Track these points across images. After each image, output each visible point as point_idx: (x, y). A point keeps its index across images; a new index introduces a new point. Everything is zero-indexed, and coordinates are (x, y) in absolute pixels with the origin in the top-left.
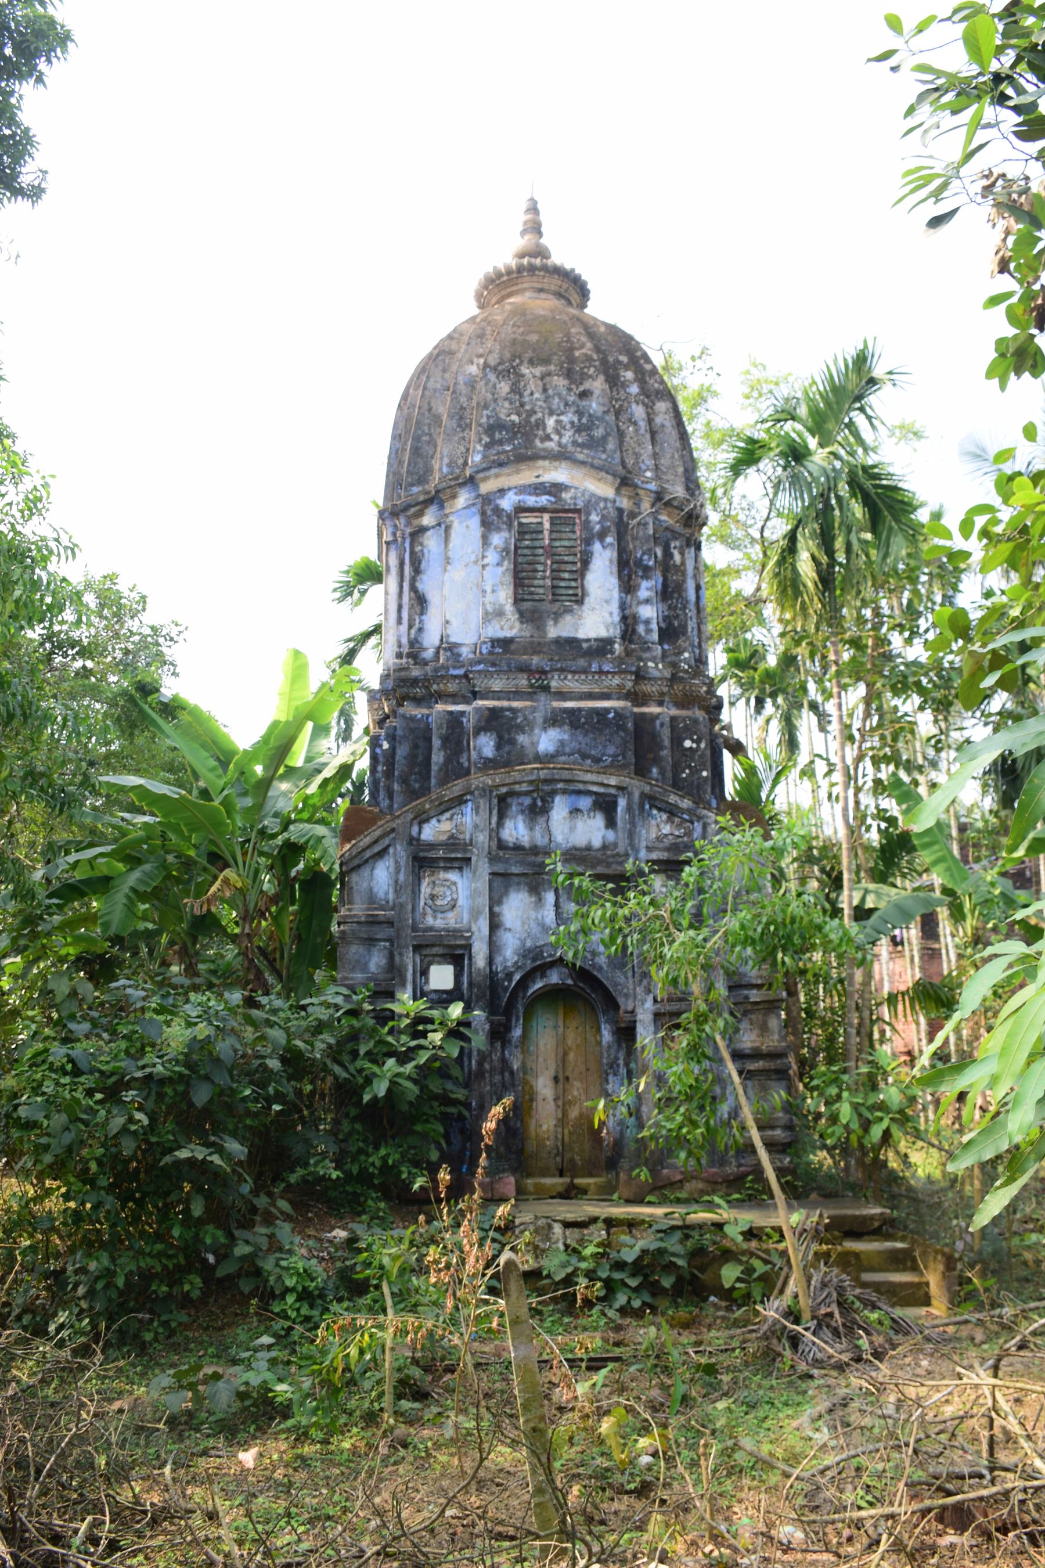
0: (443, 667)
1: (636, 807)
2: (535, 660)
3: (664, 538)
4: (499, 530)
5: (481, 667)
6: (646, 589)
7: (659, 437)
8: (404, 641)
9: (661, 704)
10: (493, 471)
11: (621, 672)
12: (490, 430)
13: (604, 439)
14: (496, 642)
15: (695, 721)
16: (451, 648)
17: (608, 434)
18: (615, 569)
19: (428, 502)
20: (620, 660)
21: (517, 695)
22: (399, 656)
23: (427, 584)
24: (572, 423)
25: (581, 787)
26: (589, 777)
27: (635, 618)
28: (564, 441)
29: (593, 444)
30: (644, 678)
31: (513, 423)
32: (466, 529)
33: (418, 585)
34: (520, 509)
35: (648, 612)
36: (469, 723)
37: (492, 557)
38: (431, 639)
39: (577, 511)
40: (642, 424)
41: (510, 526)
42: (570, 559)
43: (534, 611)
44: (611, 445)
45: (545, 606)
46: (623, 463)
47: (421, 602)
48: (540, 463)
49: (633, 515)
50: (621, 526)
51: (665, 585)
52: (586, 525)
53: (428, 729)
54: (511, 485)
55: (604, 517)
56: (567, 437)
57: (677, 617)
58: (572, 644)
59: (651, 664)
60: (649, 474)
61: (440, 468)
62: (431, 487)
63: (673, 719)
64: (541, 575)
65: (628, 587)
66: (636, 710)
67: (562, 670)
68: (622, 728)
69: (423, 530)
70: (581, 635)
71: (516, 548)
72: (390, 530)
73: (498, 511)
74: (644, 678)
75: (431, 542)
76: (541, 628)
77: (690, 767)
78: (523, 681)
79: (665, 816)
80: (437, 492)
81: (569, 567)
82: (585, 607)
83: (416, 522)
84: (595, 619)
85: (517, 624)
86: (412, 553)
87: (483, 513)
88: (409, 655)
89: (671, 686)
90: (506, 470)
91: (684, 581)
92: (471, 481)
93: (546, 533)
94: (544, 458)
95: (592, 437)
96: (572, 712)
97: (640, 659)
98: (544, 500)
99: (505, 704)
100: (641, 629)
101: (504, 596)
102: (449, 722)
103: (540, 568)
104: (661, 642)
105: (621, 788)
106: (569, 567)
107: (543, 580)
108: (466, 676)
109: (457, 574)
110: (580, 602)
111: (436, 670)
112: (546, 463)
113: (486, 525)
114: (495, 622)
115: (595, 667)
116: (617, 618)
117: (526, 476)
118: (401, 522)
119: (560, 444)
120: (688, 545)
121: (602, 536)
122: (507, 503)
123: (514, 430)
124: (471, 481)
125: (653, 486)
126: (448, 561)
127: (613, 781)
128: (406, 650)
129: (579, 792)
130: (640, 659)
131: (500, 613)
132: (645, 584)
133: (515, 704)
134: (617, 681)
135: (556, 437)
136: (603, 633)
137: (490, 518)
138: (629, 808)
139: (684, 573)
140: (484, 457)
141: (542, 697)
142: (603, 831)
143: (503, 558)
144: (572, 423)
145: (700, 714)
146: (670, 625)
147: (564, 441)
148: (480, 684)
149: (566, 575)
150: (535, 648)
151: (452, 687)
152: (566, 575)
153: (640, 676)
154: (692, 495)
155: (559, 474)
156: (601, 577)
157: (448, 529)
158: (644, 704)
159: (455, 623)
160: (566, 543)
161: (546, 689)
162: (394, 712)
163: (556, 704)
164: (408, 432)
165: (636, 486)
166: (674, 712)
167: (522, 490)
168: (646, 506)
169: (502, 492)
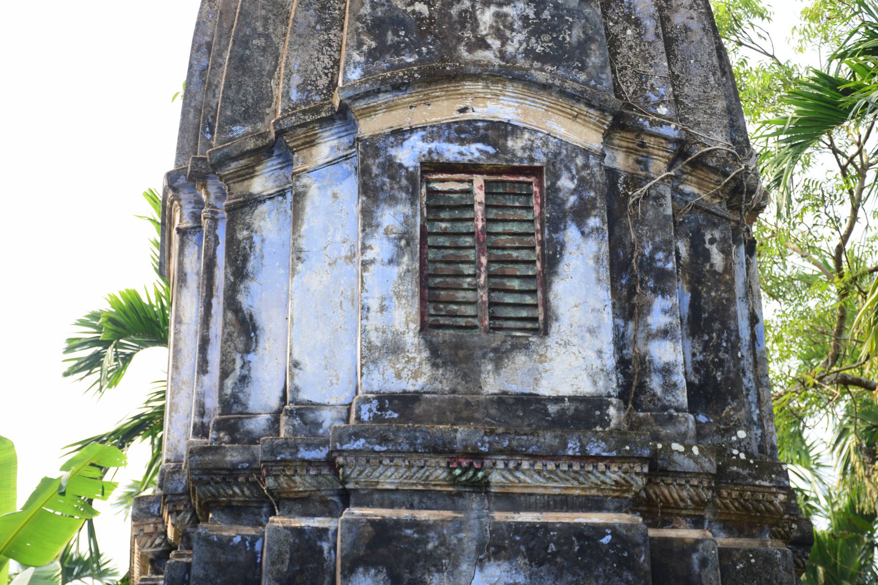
0: (286, 444)
2: (462, 433)
3: (692, 223)
4: (393, 200)
5: (360, 443)
6: (661, 312)
7: (679, 49)
8: (212, 403)
9: (698, 523)
10: (383, 98)
11: (621, 459)
12: (377, 27)
13: (583, 47)
14: (386, 400)
15: (768, 559)
16: (297, 409)
17: (589, 39)
18: (605, 274)
19: (263, 152)
20: (620, 436)
21: (426, 497)
22: (201, 430)
23: (257, 298)
24: (525, 19)
27: (644, 364)
28: (510, 49)
29: (558, 56)
30: (665, 472)
31: (418, 15)
32: (331, 199)
33: (241, 298)
34: (433, 166)
35: (667, 353)
36: (334, 552)
37: (380, 248)
38: (264, 396)
39: (536, 172)
40: (650, 24)
41: (413, 195)
42: (523, 255)
43: (457, 346)
44: (595, 59)
45: (478, 338)
46: (617, 90)
47: (245, 329)
48: (469, 86)
49: (634, 181)
50: (615, 199)
51: (695, 306)
52: (552, 196)
53: (254, 564)
54: (416, 126)
55: (583, 183)
56: (516, 43)
57: (721, 364)
58: (530, 403)
59: (676, 446)
60: (663, 110)
61: (285, 92)
62: (268, 126)
63: (724, 553)
64: (471, 286)
65: (628, 308)
66: (652, 533)
67: (511, 452)
68: (629, 564)
69: (252, 201)
70: (545, 390)
71: (424, 234)
72: (188, 209)
73: (392, 168)
74: (665, 472)
75: (268, 225)
76: (471, 376)
78: (437, 472)
80: (280, 133)
81: (522, 270)
82: (552, 340)
83: (238, 188)
84: (571, 362)
85: (427, 368)
86: (231, 241)
87: (364, 172)
88: (220, 426)
89: (717, 490)
90: (405, 98)
91: (731, 301)
92: (343, 116)
93: (479, 209)
94: (475, 78)
95: (561, 44)
96: (531, 530)
97: (656, 438)
98: (474, 151)
99: (405, 514)
100: (655, 383)
101: (403, 319)
102: (295, 549)
103: (468, 269)
104: (693, 407)
106: (522, 270)
107: (473, 295)
108: (330, 462)
109: (316, 280)
110: (543, 331)
111: (273, 450)
112: (479, 86)
113: (371, 192)
114: (384, 364)
115: (573, 447)
116: (610, 362)
117: (443, 109)
118: (208, 194)
119: (502, 55)
120: (737, 241)
121: (580, 215)
122: (408, 155)
123: (420, 29)
124: (343, 116)
125: (671, 131)
126: (298, 254)
128: (212, 419)
130: (656, 438)
131: (394, 349)
132: (659, 303)
133: (423, 515)
134: (614, 474)
135: (496, 44)
136: (586, 388)
137: (376, 178)
139: (730, 287)
140: (367, 73)
141: (474, 503)
143: (401, 251)
144: (525, 19)
145: (774, 546)
146: (708, 378)
147: (510, 49)
148: (357, 476)
149: (516, 284)
150: (460, 410)
151: (303, 483)
152: (516, 284)
153: (658, 468)
154: (741, 152)
155: (501, 106)
156: (580, 287)
157: (299, 198)
158: (664, 524)
159: (310, 366)
160: (515, 228)
161: (481, 487)
162: (185, 537)
163: (499, 516)
164: (223, 35)
165: (640, 131)
166: (724, 540)
167: (434, 132)
168: (658, 166)
169: (399, 134)
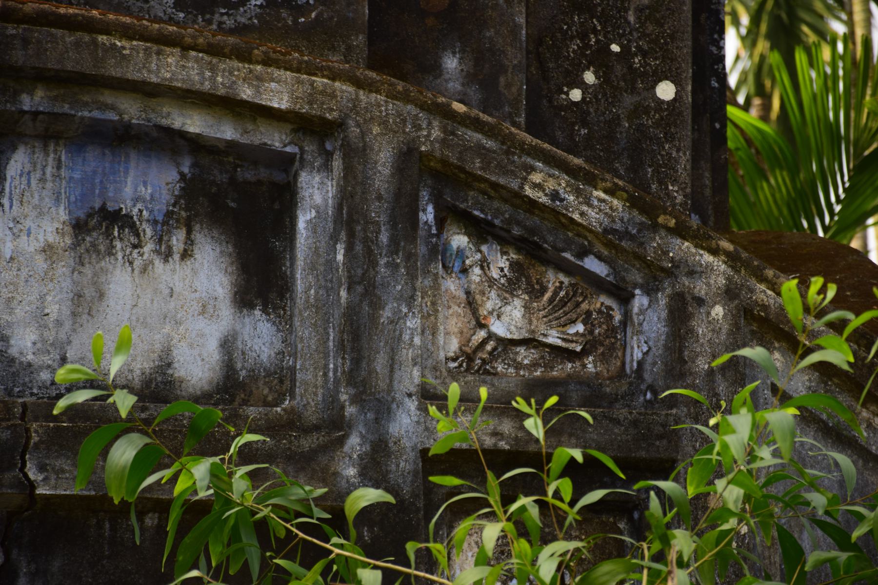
1: (378, 212)
25: (131, 110)
26: (171, 68)
77: (600, 59)
79: (500, 263)
105: (312, 127)
127: (279, 93)
129: (122, 139)
138: (348, 217)
142: (226, 312)
